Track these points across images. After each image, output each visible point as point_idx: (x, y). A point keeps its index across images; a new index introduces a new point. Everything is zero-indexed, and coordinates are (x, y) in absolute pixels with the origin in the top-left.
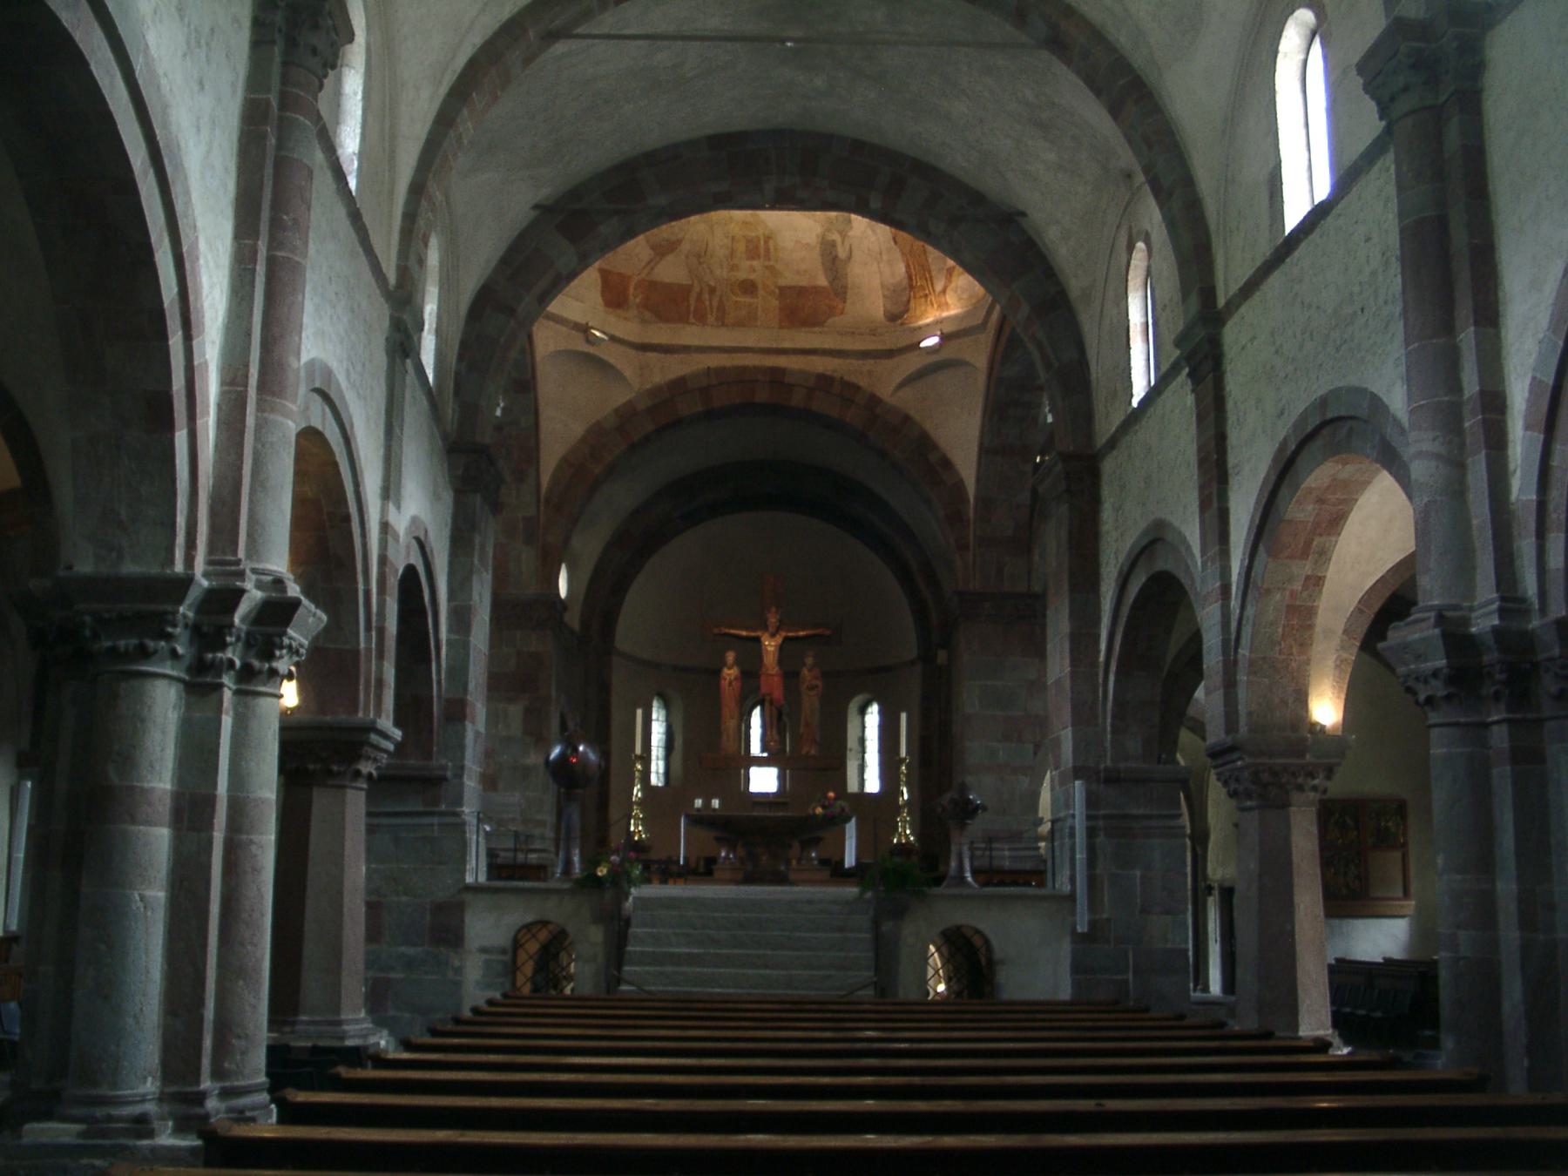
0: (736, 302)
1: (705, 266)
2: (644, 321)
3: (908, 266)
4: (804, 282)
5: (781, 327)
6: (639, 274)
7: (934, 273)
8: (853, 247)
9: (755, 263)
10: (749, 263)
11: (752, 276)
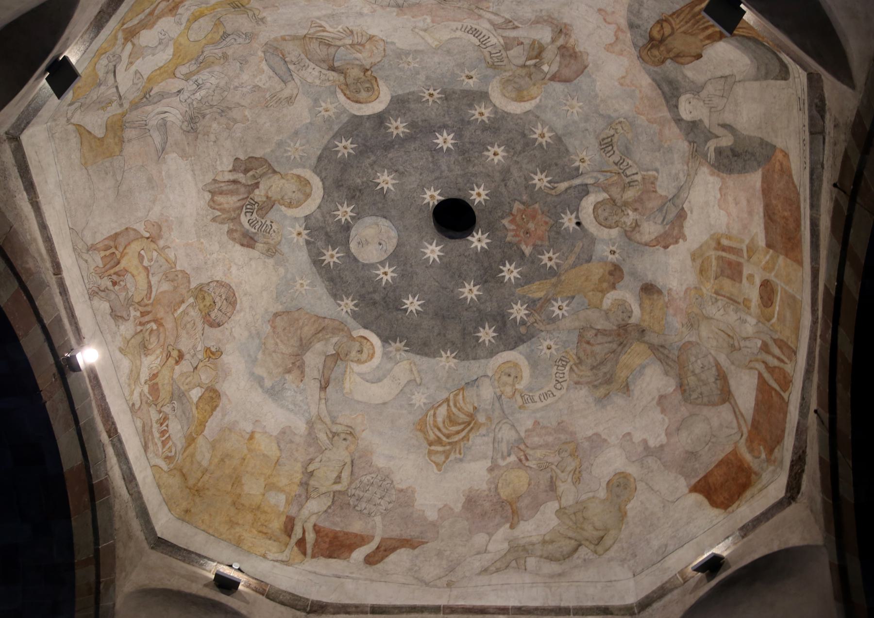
6: (742, 436)
8: (721, 122)
10: (744, 280)
11: (758, 282)
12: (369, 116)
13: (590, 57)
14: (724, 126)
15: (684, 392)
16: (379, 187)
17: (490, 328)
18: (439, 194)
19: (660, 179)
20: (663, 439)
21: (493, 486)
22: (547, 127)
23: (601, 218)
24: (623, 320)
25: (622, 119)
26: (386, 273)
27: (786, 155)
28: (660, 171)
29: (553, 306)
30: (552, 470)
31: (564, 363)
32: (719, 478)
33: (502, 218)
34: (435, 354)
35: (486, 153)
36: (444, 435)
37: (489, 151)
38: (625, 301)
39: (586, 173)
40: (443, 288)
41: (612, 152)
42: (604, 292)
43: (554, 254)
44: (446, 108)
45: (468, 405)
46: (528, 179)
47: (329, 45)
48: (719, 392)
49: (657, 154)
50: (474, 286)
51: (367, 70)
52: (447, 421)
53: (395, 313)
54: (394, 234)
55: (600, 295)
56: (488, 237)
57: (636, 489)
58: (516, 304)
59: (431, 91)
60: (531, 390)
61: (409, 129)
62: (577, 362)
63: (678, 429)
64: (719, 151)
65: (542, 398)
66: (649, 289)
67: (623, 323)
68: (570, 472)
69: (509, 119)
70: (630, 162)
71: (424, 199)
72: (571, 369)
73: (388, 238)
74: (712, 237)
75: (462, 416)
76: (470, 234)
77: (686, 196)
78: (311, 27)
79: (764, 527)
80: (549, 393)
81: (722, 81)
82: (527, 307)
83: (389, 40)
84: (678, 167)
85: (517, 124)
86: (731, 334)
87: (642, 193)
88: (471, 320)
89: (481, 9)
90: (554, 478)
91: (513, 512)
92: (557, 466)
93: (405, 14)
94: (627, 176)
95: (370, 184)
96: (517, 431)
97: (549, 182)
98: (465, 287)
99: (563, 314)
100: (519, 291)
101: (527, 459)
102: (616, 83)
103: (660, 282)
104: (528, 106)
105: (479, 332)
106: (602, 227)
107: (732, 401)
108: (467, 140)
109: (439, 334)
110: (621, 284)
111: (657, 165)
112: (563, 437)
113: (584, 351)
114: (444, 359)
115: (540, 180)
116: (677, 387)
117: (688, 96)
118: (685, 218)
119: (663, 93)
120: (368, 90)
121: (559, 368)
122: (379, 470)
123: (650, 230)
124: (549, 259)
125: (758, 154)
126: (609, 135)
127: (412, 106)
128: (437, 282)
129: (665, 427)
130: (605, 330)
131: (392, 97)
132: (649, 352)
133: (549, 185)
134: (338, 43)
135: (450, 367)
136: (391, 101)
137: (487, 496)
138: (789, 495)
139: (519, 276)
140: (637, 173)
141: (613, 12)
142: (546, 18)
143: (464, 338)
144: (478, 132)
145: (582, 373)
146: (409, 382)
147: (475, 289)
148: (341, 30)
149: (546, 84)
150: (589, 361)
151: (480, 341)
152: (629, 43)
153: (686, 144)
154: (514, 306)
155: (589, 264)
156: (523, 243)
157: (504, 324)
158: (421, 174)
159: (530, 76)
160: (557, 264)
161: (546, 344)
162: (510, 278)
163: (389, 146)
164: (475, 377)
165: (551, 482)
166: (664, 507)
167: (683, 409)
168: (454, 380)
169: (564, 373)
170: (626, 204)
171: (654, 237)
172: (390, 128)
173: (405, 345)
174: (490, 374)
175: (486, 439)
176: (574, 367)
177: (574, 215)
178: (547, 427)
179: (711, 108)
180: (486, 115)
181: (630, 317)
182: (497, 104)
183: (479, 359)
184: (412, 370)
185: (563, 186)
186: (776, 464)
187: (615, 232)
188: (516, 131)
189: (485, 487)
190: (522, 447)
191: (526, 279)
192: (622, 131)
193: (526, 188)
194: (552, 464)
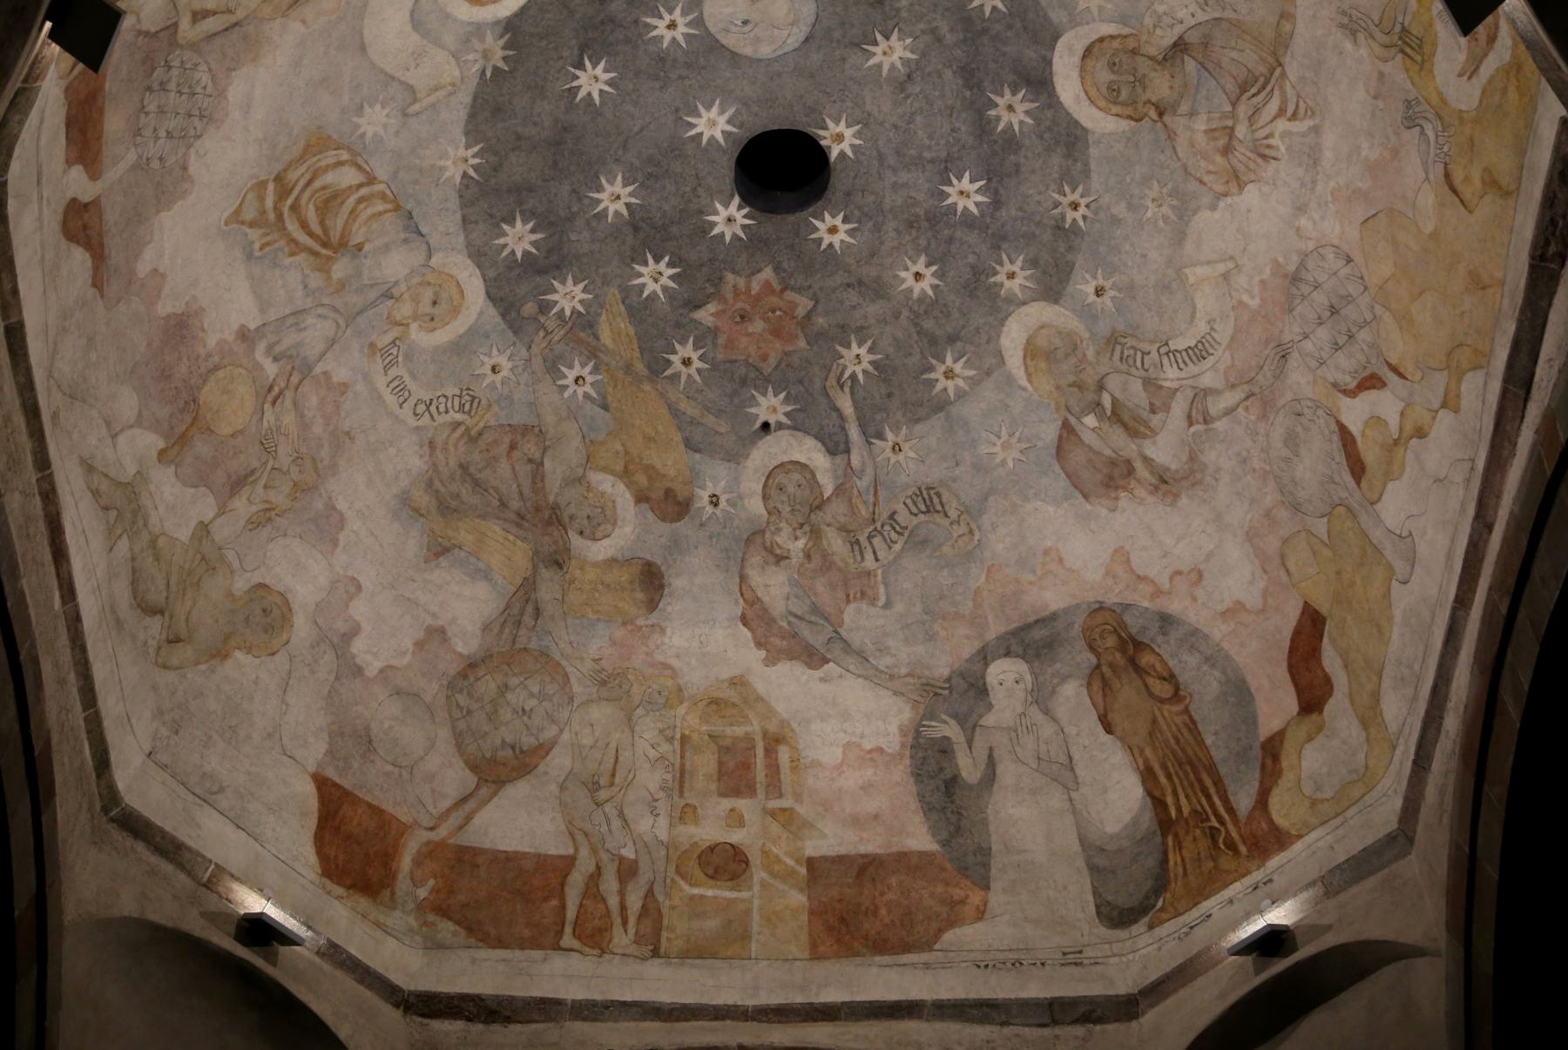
0: (692, 898)
1: (608, 808)
2: (434, 945)
3: (1147, 775)
4: (871, 844)
5: (816, 956)
6: (432, 829)
7: (1223, 770)
8: (996, 754)
9: (742, 804)
10: (727, 803)
11: (736, 837)
12: (1050, 63)
13: (1104, 511)
14: (991, 763)
15: (463, 675)
16: (879, 37)
17: (533, 243)
18: (842, 154)
19: (873, 611)
20: (373, 667)
21: (216, 359)
22: (967, 388)
23: (781, 478)
24: (572, 517)
25: (977, 537)
26: (672, 26)
27: (981, 914)
28: (888, 612)
29: (583, 365)
30: (265, 464)
31: (467, 407)
32: (355, 822)
33: (777, 269)
34: (473, 130)
35: (923, 259)
36: (297, 199)
37: (927, 266)
38: (615, 524)
39: (871, 453)
40: (626, 142)
41: (914, 510)
42: (626, 475)
43: (699, 371)
44: (1038, 218)
45: (364, 229)
46: (862, 333)
47: (1243, 89)
48: (488, 755)
49: (919, 608)
50: (628, 205)
51: (1161, 114)
52: (328, 193)
53: (574, 42)
54: (765, 51)
55: (619, 467)
56: (735, 237)
57: (273, 654)
58: (585, 290)
59: (1082, 210)
60: (408, 357)
61: (1003, 131)
62: (473, 433)
63: (398, 692)
64: (944, 749)
65: (396, 383)
66: (651, 581)
67: (567, 520)
68: (267, 502)
69: (991, 319)
70: (897, 547)
71: (837, 122)
72: (456, 425)
73: (757, 40)
74: (783, 723)
75: (340, 223)
76: (747, 200)
77: (851, 668)
78: (1299, 96)
79: (348, 983)
80: (407, 394)
81: (1063, 759)
82: (579, 313)
83: (1222, 204)
84: (901, 654)
85: (977, 330)
86: (617, 780)
87: (840, 570)
88: (550, 202)
89: (1247, 398)
90: (252, 479)
91: (183, 436)
92: (273, 469)
93: (1273, 274)
94: (870, 538)
95: (891, 23)
96: (323, 355)
97: (853, 377)
98: (625, 186)
99: (566, 387)
100: (613, 293)
101: (274, 403)
102: (1049, 544)
103: (672, 606)
104: (1014, 362)
105: (525, 222)
106: (763, 479)
107: (484, 791)
108: (958, 234)
109: (519, 137)
110: (650, 515)
111: (899, 607)
112: (325, 453)
113: (495, 441)
114: (462, 152)
115: (857, 358)
116: (469, 657)
117: (1028, 678)
118: (810, 665)
119: (1027, 627)
120: (1113, 91)
121: (457, 400)
122: (222, 93)
123: (774, 587)
124: (686, 357)
125: (961, 841)
126: (947, 508)
127: (1056, 160)
128: (642, 130)
129: (394, 662)
130: (542, 481)
131: (1085, 130)
132: (519, 581)
133: (846, 375)
134: (1243, 110)
135: (443, 169)
136: (1077, 123)
137: (198, 357)
138: (412, 999)
139: (645, 295)
140: (877, 560)
141: (1194, 599)
142: (1199, 476)
143: (509, 191)
144: (971, 259)
145: (452, 449)
146: (411, 89)
147: (620, 206)
148: (1271, 141)
149: (1057, 409)
150: (477, 457)
151: (505, 227)
152: (1129, 598)
153: (946, 672)
154: (581, 286)
155: (682, 447)
156: (720, 307)
157: (542, 272)
158: (895, 127)
159: (1078, 386)
160: (677, 376)
161: (503, 361)
162: (640, 275)
163: (970, 75)
164: (424, 230)
165: (246, 477)
166: (269, 735)
167: (435, 686)
168: (416, 182)
169: (447, 412)
170: (816, 534)
171: (760, 595)
172: (1014, 94)
173: (496, 69)
174: (434, 261)
175: (300, 293)
176: (462, 428)
177: (784, 420)
178: (339, 414)
179: (1016, 731)
180: (1008, 284)
181: (581, 533)
182: (1025, 309)
183: (465, 230)
184: (437, 90)
185: (846, 404)
186: (424, 929)
187: (756, 506)
188: (964, 327)
189: (212, 341)
190: (295, 379)
191: (640, 308)
192: (955, 535)
193: (843, 327)
194: (275, 459)
